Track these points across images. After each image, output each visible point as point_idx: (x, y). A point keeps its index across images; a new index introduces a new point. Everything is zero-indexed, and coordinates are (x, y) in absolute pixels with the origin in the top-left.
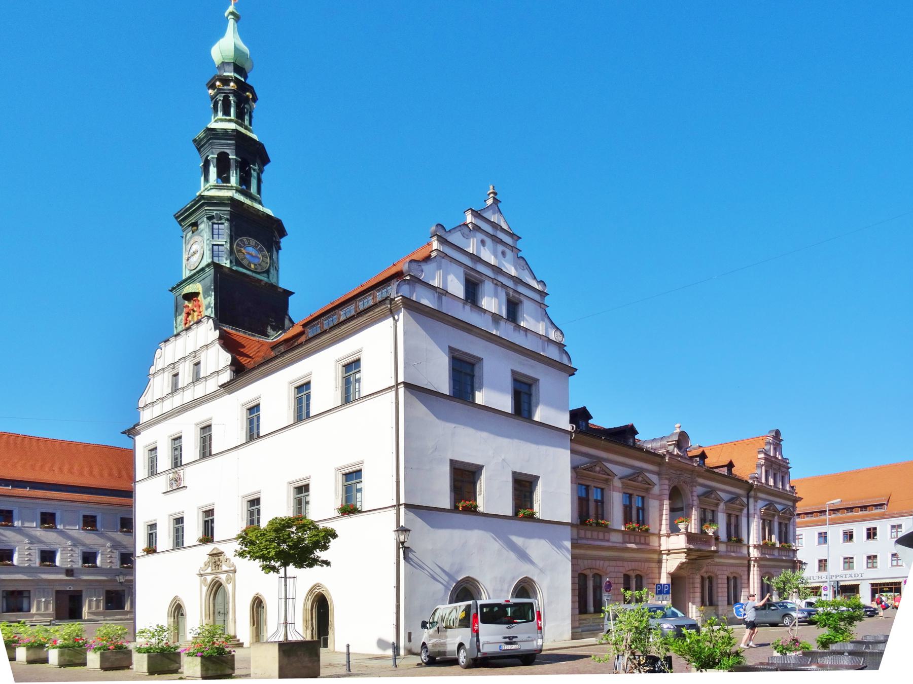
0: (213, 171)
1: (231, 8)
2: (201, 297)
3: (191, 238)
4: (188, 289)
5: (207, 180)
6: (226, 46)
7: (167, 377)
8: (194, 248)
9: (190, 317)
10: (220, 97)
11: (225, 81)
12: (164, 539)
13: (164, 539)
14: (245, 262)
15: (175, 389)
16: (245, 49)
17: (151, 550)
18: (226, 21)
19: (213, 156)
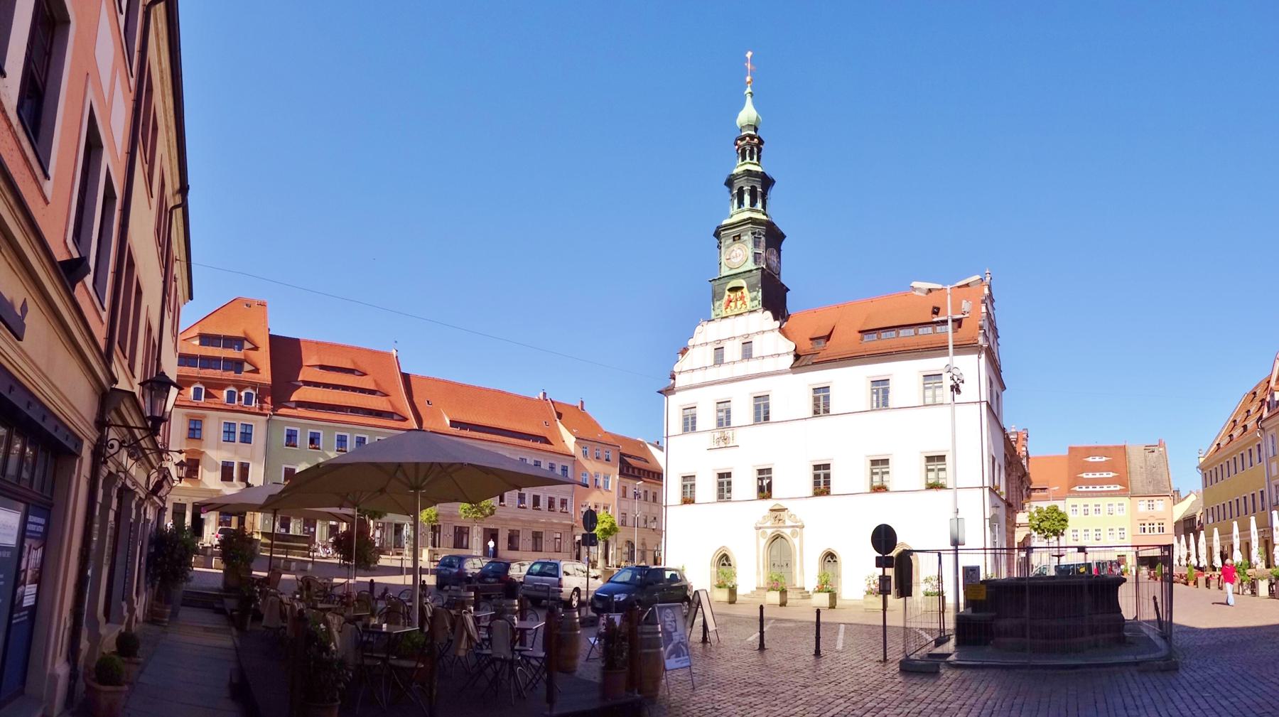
2: (745, 290)
9: (732, 304)
12: (706, 488)
13: (706, 488)
17: (688, 500)
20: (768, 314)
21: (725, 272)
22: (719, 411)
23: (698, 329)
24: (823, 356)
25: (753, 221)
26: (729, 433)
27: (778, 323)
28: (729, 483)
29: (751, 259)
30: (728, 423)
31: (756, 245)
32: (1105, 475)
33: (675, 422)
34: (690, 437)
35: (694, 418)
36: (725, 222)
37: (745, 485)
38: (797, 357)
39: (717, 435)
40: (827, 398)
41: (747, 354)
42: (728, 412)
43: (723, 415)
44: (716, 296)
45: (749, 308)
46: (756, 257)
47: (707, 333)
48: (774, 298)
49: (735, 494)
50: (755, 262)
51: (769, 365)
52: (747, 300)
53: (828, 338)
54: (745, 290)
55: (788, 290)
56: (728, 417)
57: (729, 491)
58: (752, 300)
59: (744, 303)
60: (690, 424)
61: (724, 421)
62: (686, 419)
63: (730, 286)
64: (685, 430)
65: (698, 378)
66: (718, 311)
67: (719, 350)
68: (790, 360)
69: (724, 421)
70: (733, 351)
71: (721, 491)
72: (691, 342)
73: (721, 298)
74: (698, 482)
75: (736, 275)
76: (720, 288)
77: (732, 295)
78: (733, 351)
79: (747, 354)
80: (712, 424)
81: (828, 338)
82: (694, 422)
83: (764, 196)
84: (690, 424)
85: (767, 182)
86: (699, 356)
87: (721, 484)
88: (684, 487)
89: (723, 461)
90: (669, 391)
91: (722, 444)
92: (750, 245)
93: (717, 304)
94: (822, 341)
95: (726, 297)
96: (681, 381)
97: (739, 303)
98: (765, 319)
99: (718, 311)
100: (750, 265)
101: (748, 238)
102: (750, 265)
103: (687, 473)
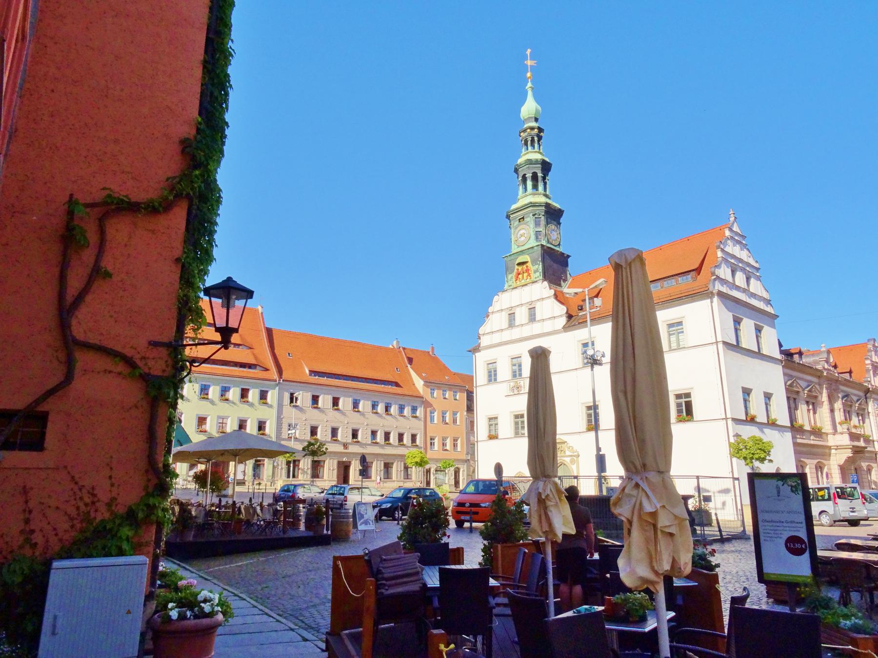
0: (529, 183)
1: (529, 85)
2: (529, 264)
3: (518, 226)
4: (521, 259)
5: (526, 189)
6: (530, 107)
7: (504, 316)
8: (522, 232)
9: (520, 276)
10: (529, 139)
11: (532, 129)
15: (512, 323)
16: (540, 108)
17: (493, 437)
18: (527, 92)
19: (529, 175)
20: (546, 283)
21: (515, 249)
23: (496, 298)
25: (533, 205)
27: (552, 292)
29: (533, 237)
30: (520, 375)
31: (537, 224)
33: (480, 377)
34: (493, 387)
35: (495, 371)
36: (514, 207)
38: (570, 317)
39: (512, 384)
41: (532, 318)
42: (520, 365)
43: (516, 368)
44: (508, 270)
45: (533, 279)
46: (537, 234)
47: (502, 301)
50: (537, 238)
51: (548, 327)
52: (532, 272)
56: (520, 370)
58: (535, 272)
59: (529, 275)
60: (492, 376)
62: (490, 372)
63: (518, 261)
64: (490, 381)
65: (497, 338)
66: (510, 283)
67: (512, 316)
68: (563, 321)
70: (522, 315)
72: (490, 309)
73: (513, 271)
74: (500, 421)
77: (520, 268)
78: (522, 315)
79: (532, 318)
82: (495, 375)
83: (544, 178)
84: (492, 376)
85: (546, 167)
86: (496, 321)
87: (516, 423)
88: (490, 425)
90: (476, 349)
91: (516, 392)
92: (532, 225)
93: (510, 276)
96: (484, 341)
97: (525, 275)
98: (543, 289)
100: (533, 243)
101: (530, 219)
102: (533, 243)
103: (492, 414)
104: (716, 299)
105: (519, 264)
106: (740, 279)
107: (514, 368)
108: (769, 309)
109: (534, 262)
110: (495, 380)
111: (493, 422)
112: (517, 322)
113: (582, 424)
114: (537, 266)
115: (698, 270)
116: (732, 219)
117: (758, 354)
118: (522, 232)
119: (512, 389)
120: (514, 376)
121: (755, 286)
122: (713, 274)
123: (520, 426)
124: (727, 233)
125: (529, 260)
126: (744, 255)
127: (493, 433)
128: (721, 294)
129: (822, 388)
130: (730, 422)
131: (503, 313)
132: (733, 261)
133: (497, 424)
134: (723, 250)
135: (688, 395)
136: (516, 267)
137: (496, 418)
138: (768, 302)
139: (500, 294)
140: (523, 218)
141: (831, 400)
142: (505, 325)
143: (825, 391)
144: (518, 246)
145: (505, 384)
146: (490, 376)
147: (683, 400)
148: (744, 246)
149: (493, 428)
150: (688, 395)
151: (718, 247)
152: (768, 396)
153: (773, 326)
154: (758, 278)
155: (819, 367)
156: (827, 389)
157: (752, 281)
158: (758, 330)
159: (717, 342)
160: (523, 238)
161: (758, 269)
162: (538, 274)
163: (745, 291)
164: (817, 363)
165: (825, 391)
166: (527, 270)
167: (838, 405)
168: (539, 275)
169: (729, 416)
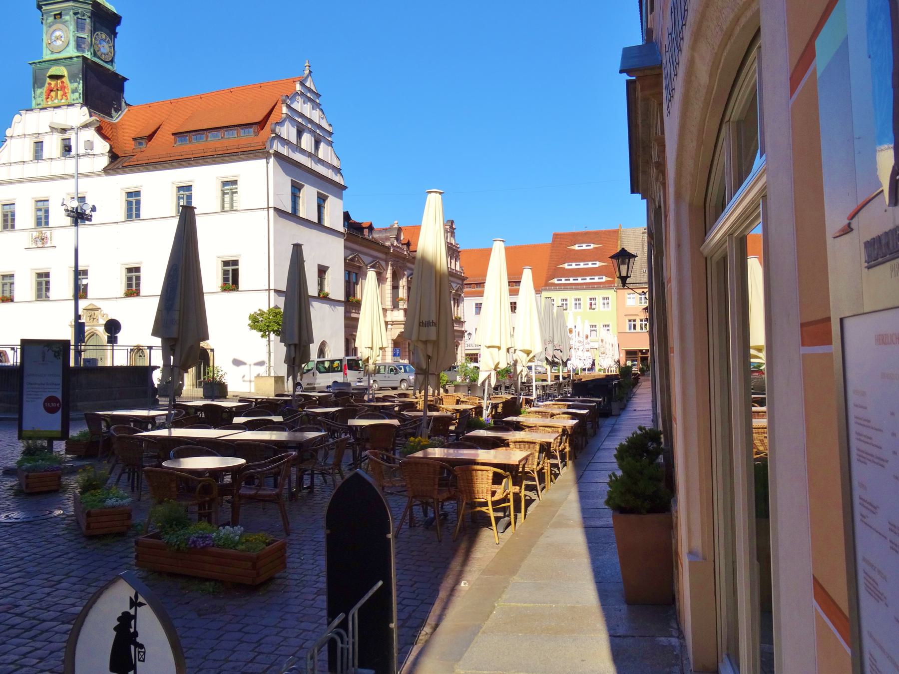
2: (66, 80)
4: (54, 70)
8: (58, 33)
9: (53, 94)
14: (99, 54)
20: (85, 109)
21: (47, 56)
22: (39, 210)
23: (17, 117)
24: (141, 157)
26: (47, 233)
28: (48, 283)
29: (73, 44)
30: (47, 223)
31: (80, 27)
32: (590, 265)
35: (13, 215)
37: (62, 285)
38: (114, 156)
39: (35, 234)
40: (138, 203)
43: (41, 214)
44: (38, 82)
48: (102, 90)
49: (52, 294)
53: (150, 137)
54: (66, 80)
55: (125, 79)
56: (47, 217)
57: (48, 289)
58: (74, 91)
59: (65, 94)
61: (42, 220)
63: (50, 73)
66: (39, 100)
67: (39, 146)
68: (105, 161)
69: (42, 220)
71: (39, 290)
72: (9, 132)
74: (16, 280)
75: (56, 62)
76: (41, 76)
77: (53, 83)
78: (53, 146)
80: (31, 222)
81: (150, 137)
82: (13, 220)
87: (39, 284)
89: (42, 260)
91: (40, 244)
92: (72, 27)
93: (39, 91)
94: (144, 141)
95: (47, 85)
97: (60, 93)
98: (79, 115)
99: (39, 100)
100: (71, 51)
102: (71, 51)
104: (272, 160)
105: (52, 77)
106: (307, 141)
107: (39, 213)
108: (337, 178)
109: (72, 78)
110: (13, 226)
111: (7, 281)
112: (46, 154)
113: (122, 288)
114: (76, 85)
115: (262, 124)
116: (307, 72)
117: (319, 225)
118: (58, 33)
119: (35, 240)
120: (39, 223)
121: (324, 152)
122: (273, 131)
123: (44, 287)
124: (298, 87)
125: (66, 74)
126: (316, 115)
127: (7, 294)
128: (278, 156)
129: (387, 265)
130: (272, 293)
131: (27, 139)
132: (300, 120)
133: (12, 284)
134: (289, 107)
135: (235, 263)
136: (48, 80)
137: (12, 276)
138: (338, 170)
139: (23, 112)
140: (60, 14)
141: (396, 277)
142: (29, 154)
143: (390, 268)
144: (52, 53)
145: (26, 233)
146: (5, 221)
147: (230, 268)
148: (316, 106)
149: (7, 288)
150: (235, 263)
151: (284, 102)
152: (322, 271)
153: (340, 197)
154: (330, 144)
155: (388, 243)
156: (392, 265)
157: (322, 145)
158: (322, 199)
159: (268, 208)
160: (59, 43)
161: (331, 134)
162: (77, 95)
163: (310, 155)
164: (388, 239)
165: (390, 268)
166: (63, 88)
167: (403, 282)
168: (78, 97)
169: (272, 287)
